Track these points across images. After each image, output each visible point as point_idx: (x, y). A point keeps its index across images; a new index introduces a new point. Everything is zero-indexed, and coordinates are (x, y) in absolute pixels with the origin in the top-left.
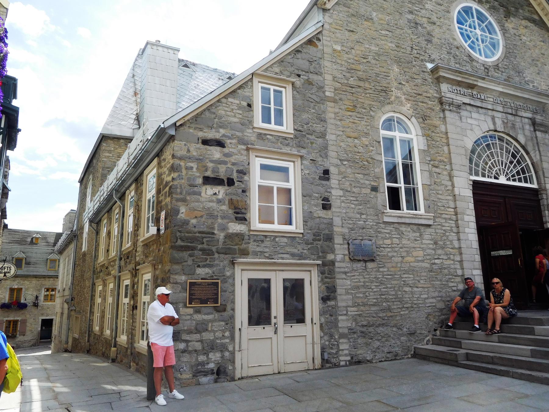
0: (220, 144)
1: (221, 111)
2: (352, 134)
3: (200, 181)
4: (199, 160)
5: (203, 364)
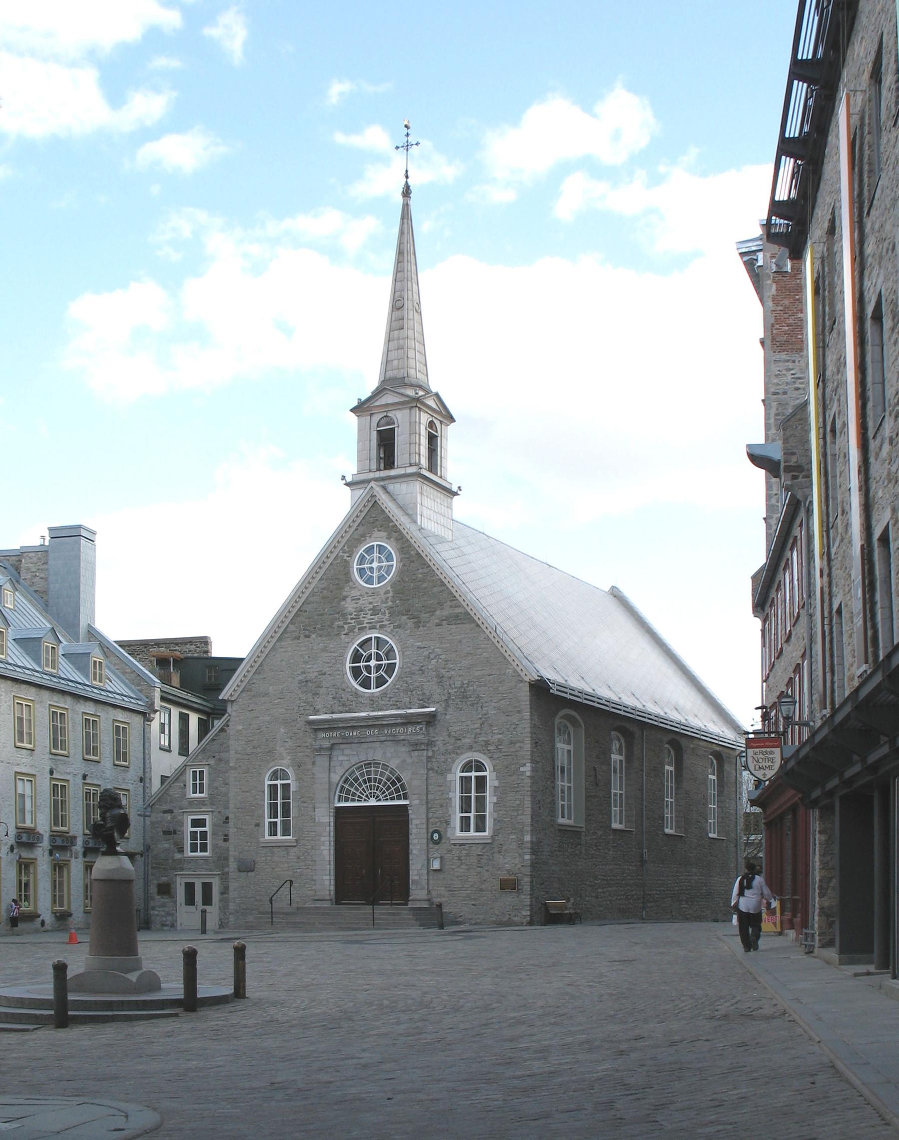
0: (170, 811)
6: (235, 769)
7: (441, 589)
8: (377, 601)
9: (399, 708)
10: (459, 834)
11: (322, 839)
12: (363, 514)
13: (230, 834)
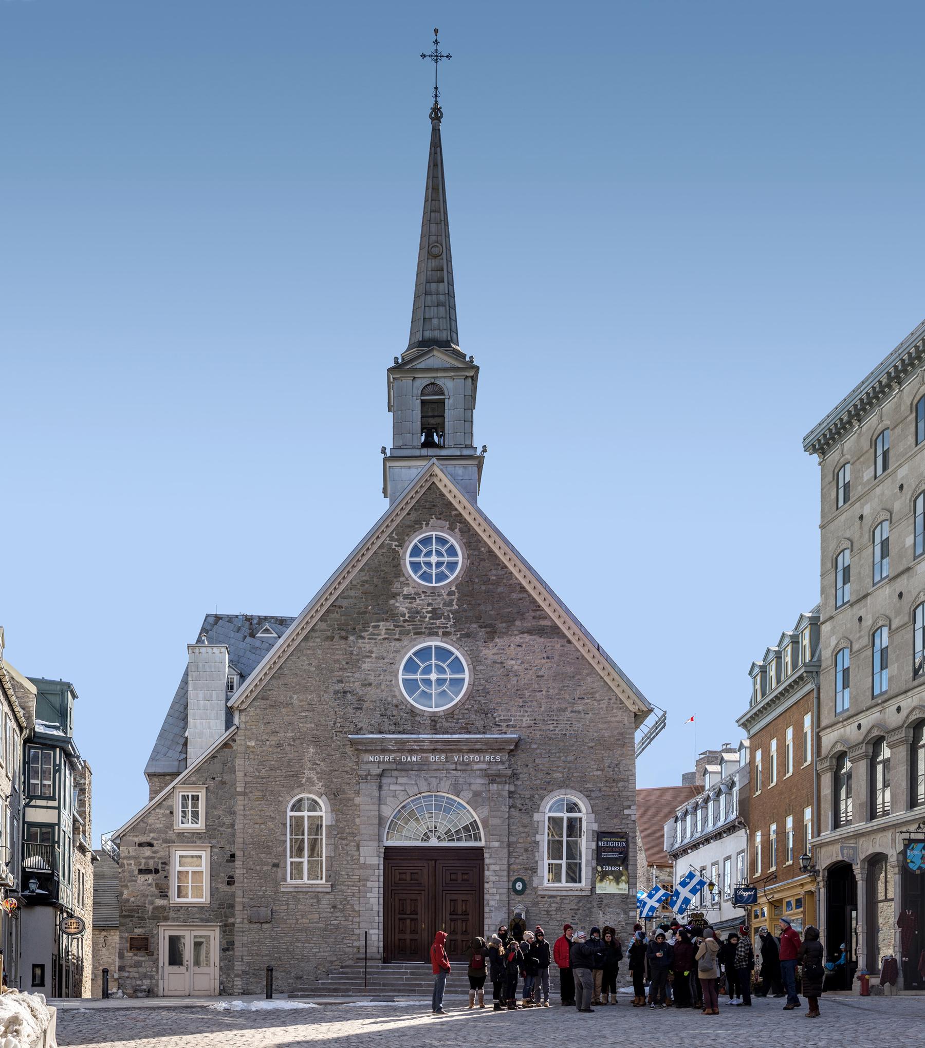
0: (150, 845)
1: (151, 820)
2: (260, 821)
3: (136, 872)
4: (135, 858)
5: (139, 986)
6: (244, 794)
7: (521, 596)
8: (439, 603)
9: (470, 733)
10: (546, 884)
11: (369, 884)
12: (419, 496)
13: (236, 876)
